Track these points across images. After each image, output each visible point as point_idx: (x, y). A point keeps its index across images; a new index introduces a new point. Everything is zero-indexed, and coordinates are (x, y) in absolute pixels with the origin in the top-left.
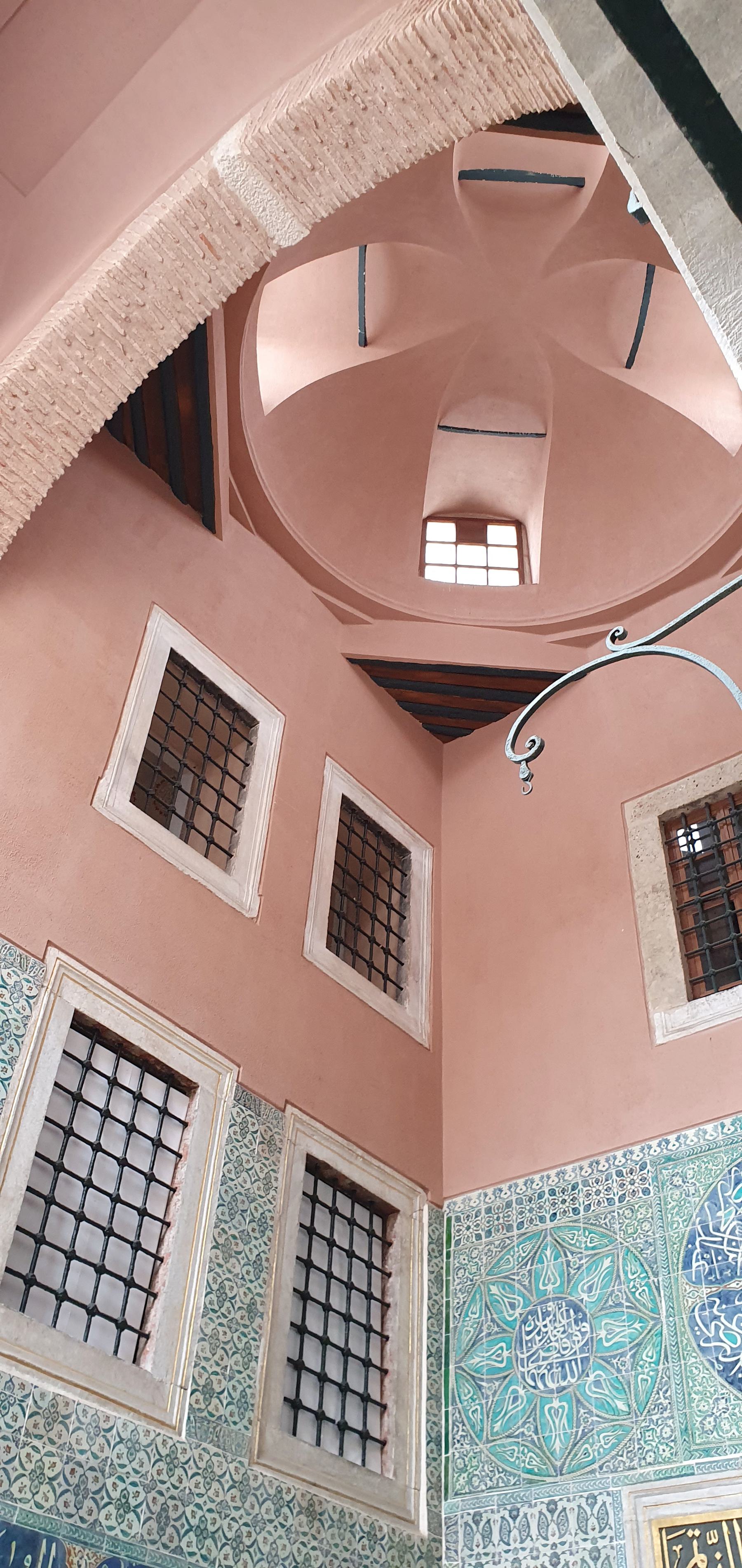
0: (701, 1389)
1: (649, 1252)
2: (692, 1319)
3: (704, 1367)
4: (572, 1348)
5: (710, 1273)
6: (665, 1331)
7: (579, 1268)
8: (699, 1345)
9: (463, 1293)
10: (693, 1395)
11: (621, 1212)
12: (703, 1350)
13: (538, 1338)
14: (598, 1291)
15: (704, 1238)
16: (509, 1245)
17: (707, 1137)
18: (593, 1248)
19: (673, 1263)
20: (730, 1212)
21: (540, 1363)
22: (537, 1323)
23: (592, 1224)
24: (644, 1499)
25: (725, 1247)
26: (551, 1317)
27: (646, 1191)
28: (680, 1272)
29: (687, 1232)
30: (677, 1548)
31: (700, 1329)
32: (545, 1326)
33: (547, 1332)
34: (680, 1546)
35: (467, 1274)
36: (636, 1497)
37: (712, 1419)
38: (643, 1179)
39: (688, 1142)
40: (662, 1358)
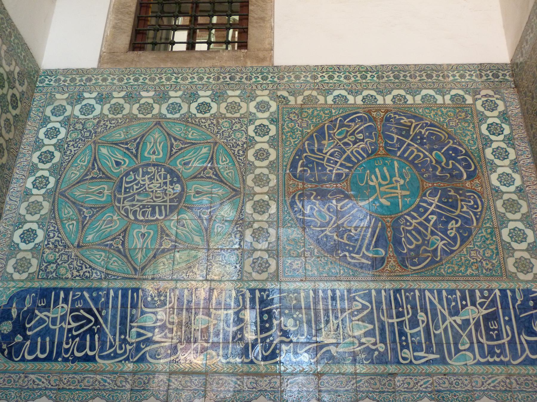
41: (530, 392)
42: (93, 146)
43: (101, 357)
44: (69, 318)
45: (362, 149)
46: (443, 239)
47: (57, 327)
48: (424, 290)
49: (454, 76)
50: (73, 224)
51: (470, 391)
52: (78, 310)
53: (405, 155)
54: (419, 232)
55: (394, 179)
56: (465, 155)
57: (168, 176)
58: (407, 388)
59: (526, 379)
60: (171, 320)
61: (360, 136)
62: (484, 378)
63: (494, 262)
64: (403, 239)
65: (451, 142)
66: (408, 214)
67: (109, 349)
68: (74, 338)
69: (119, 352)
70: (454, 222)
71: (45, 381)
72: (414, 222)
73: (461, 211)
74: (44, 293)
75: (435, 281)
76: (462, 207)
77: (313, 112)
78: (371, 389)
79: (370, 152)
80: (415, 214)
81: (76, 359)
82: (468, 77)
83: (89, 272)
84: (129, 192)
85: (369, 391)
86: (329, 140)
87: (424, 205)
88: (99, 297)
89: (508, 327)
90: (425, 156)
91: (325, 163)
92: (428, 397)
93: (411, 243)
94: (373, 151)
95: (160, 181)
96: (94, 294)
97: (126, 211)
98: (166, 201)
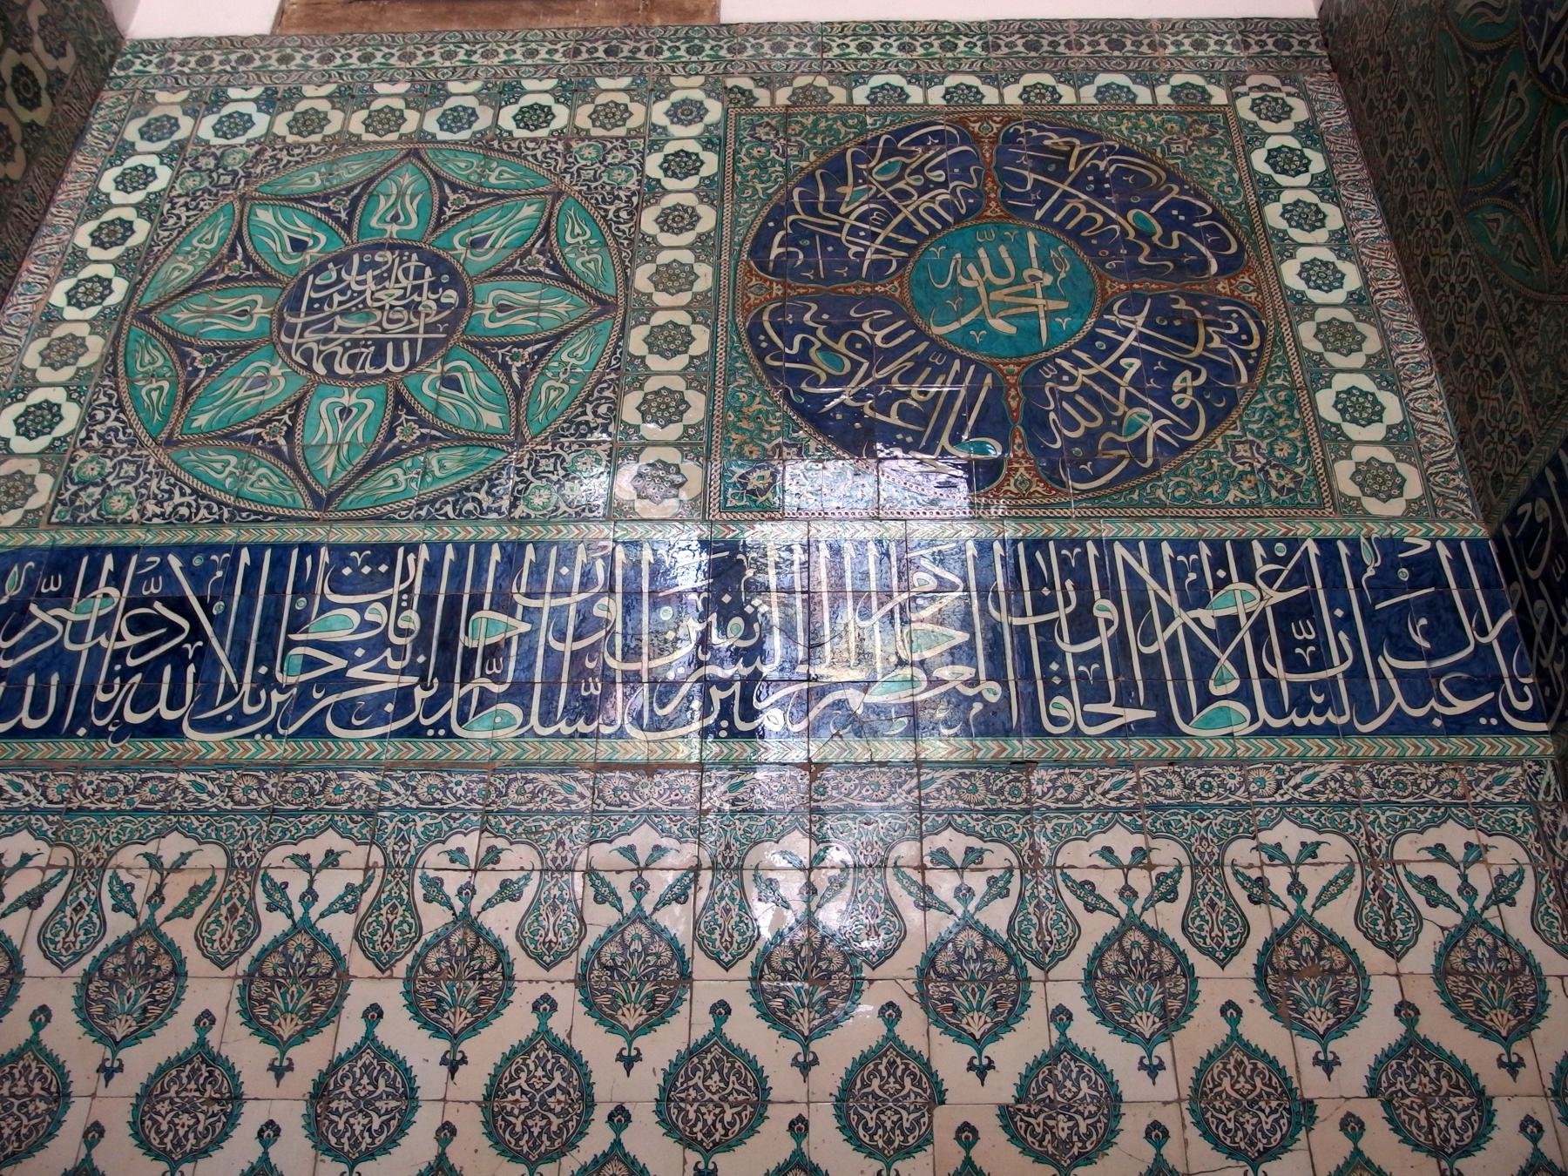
41: (1409, 805)
42: (237, 205)
43: (197, 725)
44: (120, 624)
46: (1158, 416)
47: (84, 648)
48: (1110, 542)
49: (1178, 44)
50: (161, 389)
51: (1243, 807)
52: (147, 602)
53: (1057, 219)
54: (1095, 399)
56: (1210, 218)
57: (428, 271)
58: (1065, 800)
59: (1398, 772)
60: (402, 624)
61: (939, 176)
62: (1282, 772)
63: (1299, 470)
64: (1052, 416)
65: (1176, 189)
66: (1066, 355)
67: (223, 702)
68: (126, 674)
69: (248, 709)
70: (1187, 374)
71: (32, 790)
72: (1081, 373)
73: (1205, 349)
74: (61, 562)
75: (1142, 519)
76: (1209, 339)
77: (815, 123)
78: (961, 804)
80: (1084, 356)
81: (126, 731)
82: (1213, 47)
83: (189, 506)
84: (321, 310)
85: (955, 808)
86: (856, 184)
87: (1109, 333)
88: (209, 568)
89: (1343, 636)
90: (1108, 220)
91: (844, 236)
92: (1124, 825)
93: (1074, 426)
94: (971, 210)
96: (197, 561)
97: (308, 355)
98: (415, 330)
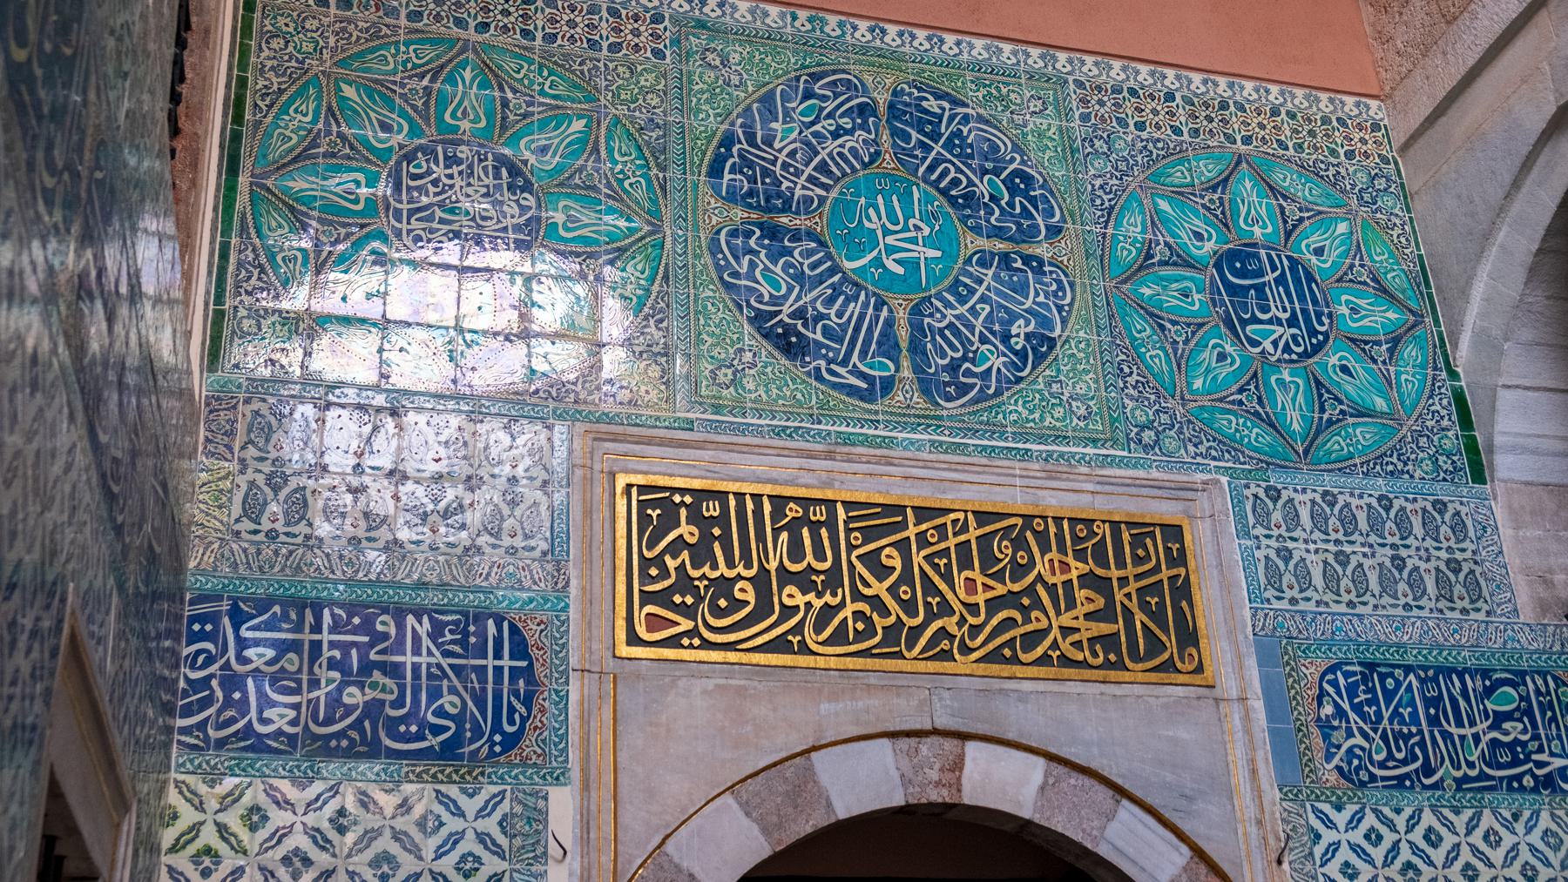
0: (717, 331)
1: (654, 135)
2: (714, 241)
3: (726, 306)
4: (499, 221)
5: (751, 193)
6: (668, 245)
7: (525, 116)
8: (721, 278)
9: (277, 76)
10: (705, 336)
11: (611, 66)
12: (728, 287)
13: (432, 189)
14: (557, 158)
15: (746, 146)
16: (386, 36)
17: (768, 21)
18: (554, 97)
19: (692, 163)
20: (791, 130)
21: (435, 225)
22: (434, 168)
23: (555, 63)
24: (607, 445)
25: (778, 169)
26: (463, 167)
27: (658, 54)
28: (702, 178)
29: (719, 134)
30: (655, 514)
31: (725, 258)
32: (451, 177)
33: (452, 187)
34: (658, 511)
35: (290, 49)
36: (595, 439)
37: (729, 372)
38: (656, 36)
39: (737, 15)
40: (659, 277)
45: (852, 149)
54: (957, 333)
55: (912, 222)
64: (929, 346)
70: (1021, 322)
72: (949, 312)
73: (1034, 302)
76: (1037, 294)
79: (866, 160)
80: (951, 298)
87: (968, 281)
93: (943, 355)
95: (487, 181)
